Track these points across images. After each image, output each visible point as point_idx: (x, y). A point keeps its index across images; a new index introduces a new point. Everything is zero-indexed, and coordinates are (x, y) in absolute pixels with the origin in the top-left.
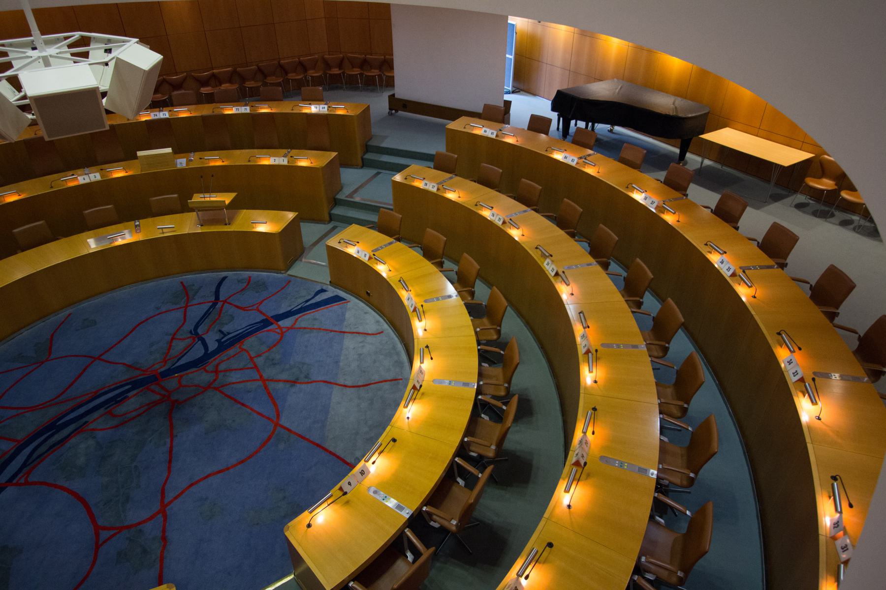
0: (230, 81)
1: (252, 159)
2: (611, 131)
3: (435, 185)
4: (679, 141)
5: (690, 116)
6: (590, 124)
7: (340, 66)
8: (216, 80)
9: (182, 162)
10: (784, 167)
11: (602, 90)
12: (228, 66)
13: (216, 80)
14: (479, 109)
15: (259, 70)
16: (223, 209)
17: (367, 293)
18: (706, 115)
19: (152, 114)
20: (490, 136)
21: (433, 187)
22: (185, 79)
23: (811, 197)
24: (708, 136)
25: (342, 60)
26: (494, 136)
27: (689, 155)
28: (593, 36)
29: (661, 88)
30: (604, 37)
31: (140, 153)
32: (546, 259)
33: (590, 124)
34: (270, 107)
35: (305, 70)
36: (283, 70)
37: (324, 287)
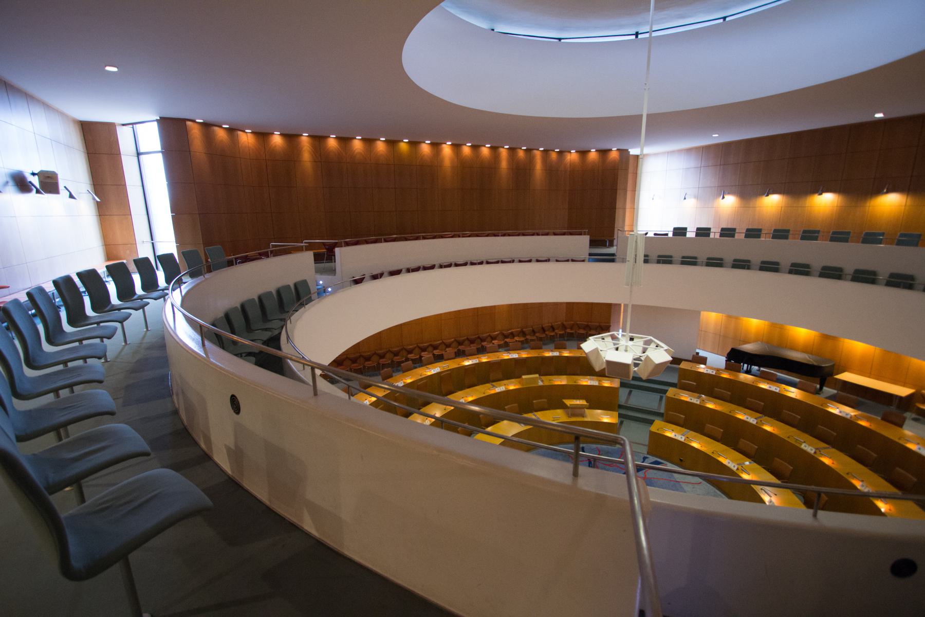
0: (518, 336)
2: (759, 370)
4: (818, 380)
5: (827, 365)
7: (572, 329)
8: (512, 335)
9: (540, 383)
10: (901, 398)
11: (749, 347)
12: (518, 328)
13: (512, 335)
14: (690, 358)
15: (533, 331)
17: (681, 460)
18: (833, 366)
20: (711, 373)
22: (498, 335)
23: (918, 414)
25: (573, 325)
26: (714, 373)
27: (825, 388)
28: (736, 318)
29: (793, 348)
30: (745, 319)
31: (524, 377)
32: (801, 445)
34: (569, 353)
36: (543, 330)
37: (646, 456)
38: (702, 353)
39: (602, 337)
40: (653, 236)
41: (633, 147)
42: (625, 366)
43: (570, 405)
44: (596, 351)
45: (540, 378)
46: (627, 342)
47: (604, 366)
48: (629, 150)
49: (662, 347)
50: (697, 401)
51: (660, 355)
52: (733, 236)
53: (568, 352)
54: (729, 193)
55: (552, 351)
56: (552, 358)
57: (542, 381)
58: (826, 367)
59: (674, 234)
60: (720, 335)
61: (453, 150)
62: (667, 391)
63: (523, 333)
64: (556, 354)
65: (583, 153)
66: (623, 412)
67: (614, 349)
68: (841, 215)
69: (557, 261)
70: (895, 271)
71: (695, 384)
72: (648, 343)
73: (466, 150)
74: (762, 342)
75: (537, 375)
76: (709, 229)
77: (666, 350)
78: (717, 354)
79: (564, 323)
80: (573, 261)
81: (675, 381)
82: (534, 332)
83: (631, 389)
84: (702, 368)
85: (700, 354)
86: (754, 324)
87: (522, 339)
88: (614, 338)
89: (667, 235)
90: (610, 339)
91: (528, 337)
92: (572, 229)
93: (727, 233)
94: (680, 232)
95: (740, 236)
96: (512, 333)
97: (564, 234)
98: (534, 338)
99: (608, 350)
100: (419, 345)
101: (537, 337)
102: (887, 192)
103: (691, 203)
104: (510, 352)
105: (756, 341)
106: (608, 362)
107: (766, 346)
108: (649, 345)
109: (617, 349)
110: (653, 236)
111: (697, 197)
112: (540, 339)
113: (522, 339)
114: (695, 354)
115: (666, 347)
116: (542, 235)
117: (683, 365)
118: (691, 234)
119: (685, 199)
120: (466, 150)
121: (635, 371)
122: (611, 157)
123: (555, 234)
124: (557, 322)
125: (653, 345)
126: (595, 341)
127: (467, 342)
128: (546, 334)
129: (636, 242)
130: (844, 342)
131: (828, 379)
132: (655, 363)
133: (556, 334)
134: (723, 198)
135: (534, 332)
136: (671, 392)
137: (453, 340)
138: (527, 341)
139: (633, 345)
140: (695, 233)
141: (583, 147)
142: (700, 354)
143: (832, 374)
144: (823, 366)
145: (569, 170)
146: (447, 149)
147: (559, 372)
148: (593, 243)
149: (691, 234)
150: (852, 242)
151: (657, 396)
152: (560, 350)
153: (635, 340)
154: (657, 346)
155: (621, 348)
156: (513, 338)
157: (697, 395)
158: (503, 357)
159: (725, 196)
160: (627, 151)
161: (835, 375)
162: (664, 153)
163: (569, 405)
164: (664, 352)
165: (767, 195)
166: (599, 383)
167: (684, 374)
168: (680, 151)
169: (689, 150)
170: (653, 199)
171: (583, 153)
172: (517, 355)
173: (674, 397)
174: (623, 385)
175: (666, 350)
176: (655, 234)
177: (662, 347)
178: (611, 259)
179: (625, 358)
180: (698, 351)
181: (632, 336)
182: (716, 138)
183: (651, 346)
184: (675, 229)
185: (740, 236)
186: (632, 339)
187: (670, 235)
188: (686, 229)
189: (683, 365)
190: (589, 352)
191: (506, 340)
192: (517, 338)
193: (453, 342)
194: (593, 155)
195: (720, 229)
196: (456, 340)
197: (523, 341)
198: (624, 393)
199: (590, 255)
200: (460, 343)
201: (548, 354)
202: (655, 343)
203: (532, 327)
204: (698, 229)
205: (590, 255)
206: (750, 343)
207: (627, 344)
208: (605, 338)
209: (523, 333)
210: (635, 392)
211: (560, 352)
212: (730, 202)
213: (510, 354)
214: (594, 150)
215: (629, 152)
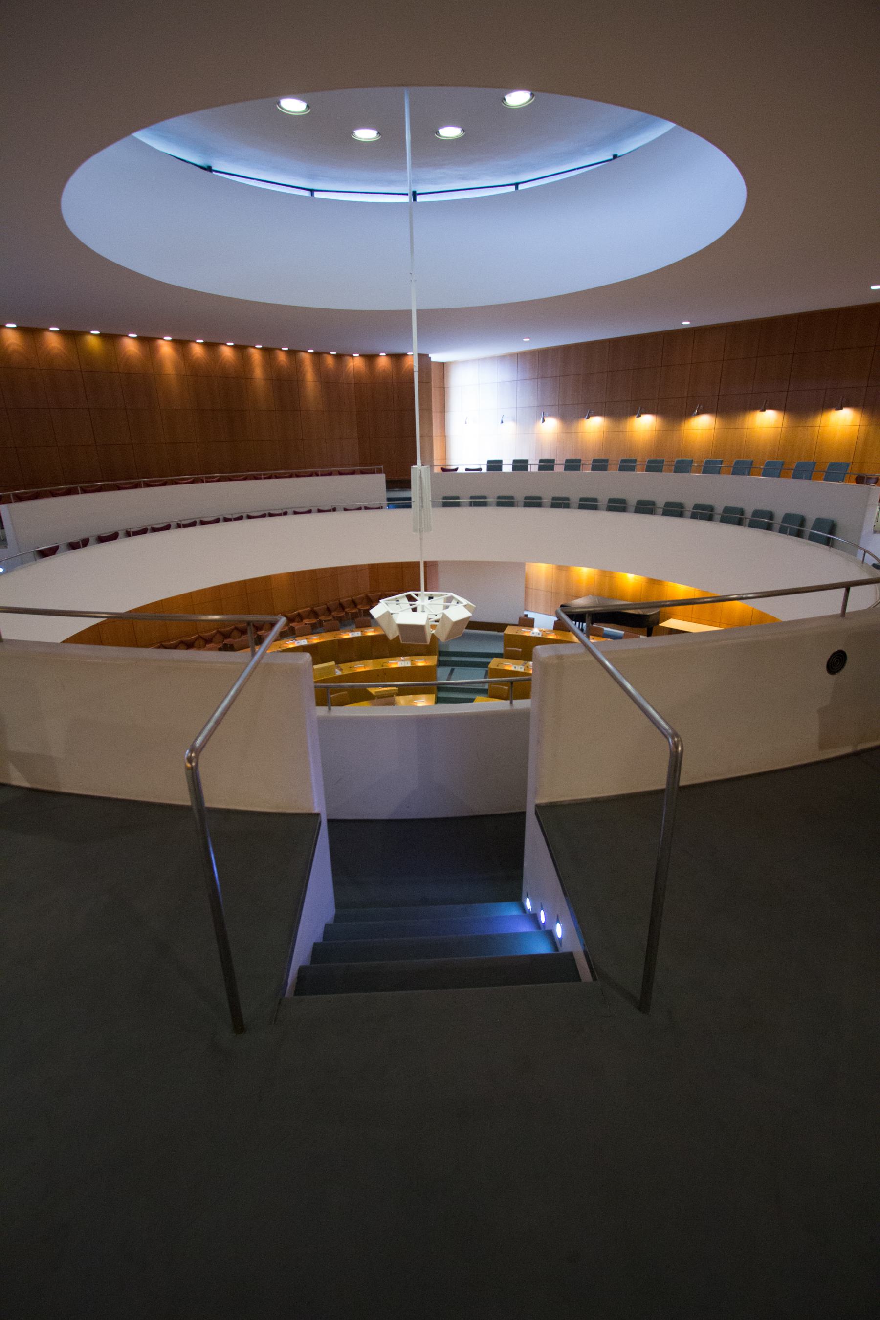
0: (308, 617)
1: (384, 664)
3: (521, 667)
5: (652, 613)
6: (581, 623)
8: (300, 617)
11: (581, 603)
13: (300, 617)
14: (517, 622)
16: (393, 696)
19: (296, 642)
21: (521, 668)
24: (663, 624)
33: (581, 623)
34: (374, 631)
35: (356, 605)
36: (342, 607)
38: (531, 615)
39: (396, 599)
40: (464, 471)
41: (435, 352)
42: (421, 628)
43: (376, 692)
44: (388, 615)
45: (338, 667)
46: (423, 601)
47: (398, 633)
48: (430, 356)
49: (462, 603)
50: (521, 668)
51: (459, 612)
52: (552, 468)
53: (372, 630)
54: (550, 415)
55: (352, 631)
56: (351, 640)
57: (341, 670)
58: (652, 615)
59: (489, 469)
60: (552, 592)
61: (176, 350)
62: (489, 663)
63: (314, 614)
64: (358, 634)
65: (370, 358)
66: (442, 695)
67: (411, 610)
68: (661, 440)
69: (345, 510)
70: (671, 500)
71: (520, 650)
72: (449, 600)
73: (197, 349)
74: (593, 595)
75: (333, 663)
76: (526, 461)
77: (465, 606)
78: (550, 615)
79: (369, 595)
80: (366, 508)
81: (500, 649)
82: (329, 610)
83: (453, 668)
84: (526, 632)
85: (529, 616)
86: (585, 573)
87: (314, 621)
88: (410, 598)
89: (480, 469)
90: (406, 600)
91: (322, 618)
92: (365, 467)
93: (546, 465)
94: (495, 465)
95: (559, 469)
96: (299, 615)
97: (353, 473)
98: (331, 618)
99: (400, 613)
100: (163, 644)
101: (334, 617)
102: (698, 414)
103: (510, 427)
104: (296, 638)
105: (587, 595)
106: (402, 627)
107: (597, 600)
108: (451, 603)
109: (414, 610)
110: (464, 471)
111: (515, 420)
112: (340, 619)
113: (314, 621)
114: (523, 616)
115: (465, 602)
116: (322, 475)
117: (509, 631)
118: (507, 468)
119: (502, 422)
120: (197, 349)
121: (433, 635)
122: (407, 365)
123: (341, 473)
124: (359, 594)
125: (454, 602)
126: (386, 604)
127: (235, 633)
128: (346, 613)
129: (421, 477)
130: (668, 586)
131: (655, 628)
132: (452, 621)
133: (360, 610)
134: (544, 421)
135: (329, 610)
136: (494, 663)
137: (215, 631)
138: (320, 624)
139: (430, 604)
140: (512, 466)
141: (370, 349)
142: (529, 616)
143: (658, 623)
144: (649, 614)
145: (353, 382)
146: (165, 348)
147: (362, 657)
148: (391, 485)
149: (507, 468)
150: (664, 472)
151: (482, 671)
152: (362, 629)
153: (434, 599)
154: (457, 603)
155: (419, 609)
156: (302, 620)
157: (522, 662)
158: (287, 645)
159: (545, 419)
160: (428, 355)
161: (661, 623)
162: (473, 361)
163: (374, 693)
164: (463, 607)
165: (588, 418)
166: (412, 664)
167: (510, 640)
168: (492, 358)
169: (502, 358)
170: (466, 423)
171: (370, 358)
172: (305, 641)
173: (497, 668)
174: (440, 664)
175: (465, 606)
176: (467, 470)
177: (462, 603)
178: (406, 504)
179: (418, 619)
180: (526, 613)
181: (431, 595)
182: (528, 344)
183: (451, 604)
184: (489, 462)
185: (559, 469)
186: (431, 598)
187: (484, 470)
188: (500, 462)
189: (509, 631)
190: (378, 618)
191: (291, 625)
192: (306, 621)
193: (214, 636)
194: (383, 361)
195: (538, 461)
196: (219, 632)
197: (315, 623)
198: (442, 672)
199: (389, 499)
200: (226, 636)
201: (347, 635)
202: (456, 599)
203: (326, 604)
204: (515, 461)
205: (389, 499)
206: (580, 597)
207: (423, 604)
208: (400, 600)
209: (314, 614)
210: (457, 670)
211: (362, 631)
212: (551, 426)
213: (296, 640)
214: (384, 354)
215: (430, 358)
